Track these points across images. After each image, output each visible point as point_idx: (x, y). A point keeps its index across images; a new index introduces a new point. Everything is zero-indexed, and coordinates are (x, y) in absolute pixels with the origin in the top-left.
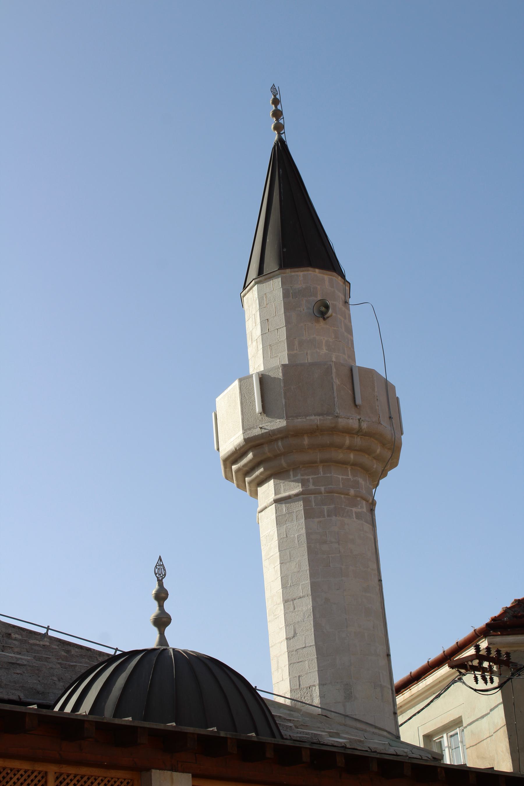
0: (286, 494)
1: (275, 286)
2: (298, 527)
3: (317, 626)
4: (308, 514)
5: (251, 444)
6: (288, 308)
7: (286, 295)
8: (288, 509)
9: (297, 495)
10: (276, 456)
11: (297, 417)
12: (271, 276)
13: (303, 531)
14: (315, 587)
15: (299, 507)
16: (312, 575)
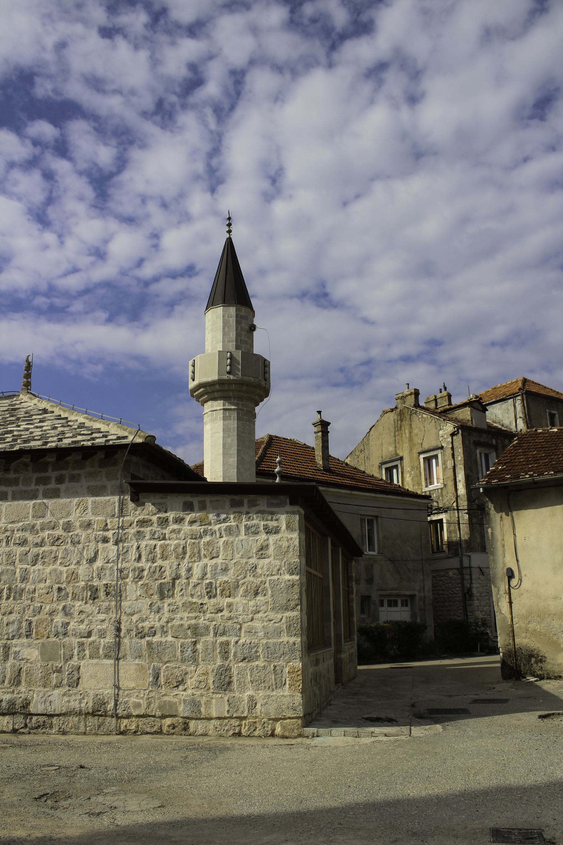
0: (229, 407)
1: (232, 310)
2: (233, 424)
3: (238, 468)
4: (239, 419)
5: (220, 382)
6: (238, 322)
7: (237, 316)
8: (229, 414)
9: (234, 409)
10: (228, 390)
11: (245, 376)
12: (230, 305)
13: (236, 425)
14: (239, 451)
15: (235, 414)
16: (238, 446)
